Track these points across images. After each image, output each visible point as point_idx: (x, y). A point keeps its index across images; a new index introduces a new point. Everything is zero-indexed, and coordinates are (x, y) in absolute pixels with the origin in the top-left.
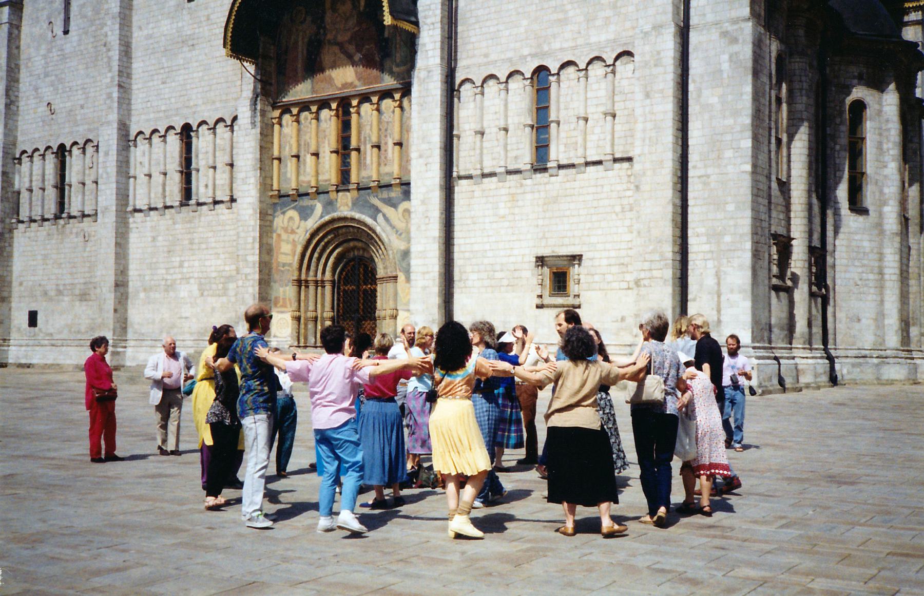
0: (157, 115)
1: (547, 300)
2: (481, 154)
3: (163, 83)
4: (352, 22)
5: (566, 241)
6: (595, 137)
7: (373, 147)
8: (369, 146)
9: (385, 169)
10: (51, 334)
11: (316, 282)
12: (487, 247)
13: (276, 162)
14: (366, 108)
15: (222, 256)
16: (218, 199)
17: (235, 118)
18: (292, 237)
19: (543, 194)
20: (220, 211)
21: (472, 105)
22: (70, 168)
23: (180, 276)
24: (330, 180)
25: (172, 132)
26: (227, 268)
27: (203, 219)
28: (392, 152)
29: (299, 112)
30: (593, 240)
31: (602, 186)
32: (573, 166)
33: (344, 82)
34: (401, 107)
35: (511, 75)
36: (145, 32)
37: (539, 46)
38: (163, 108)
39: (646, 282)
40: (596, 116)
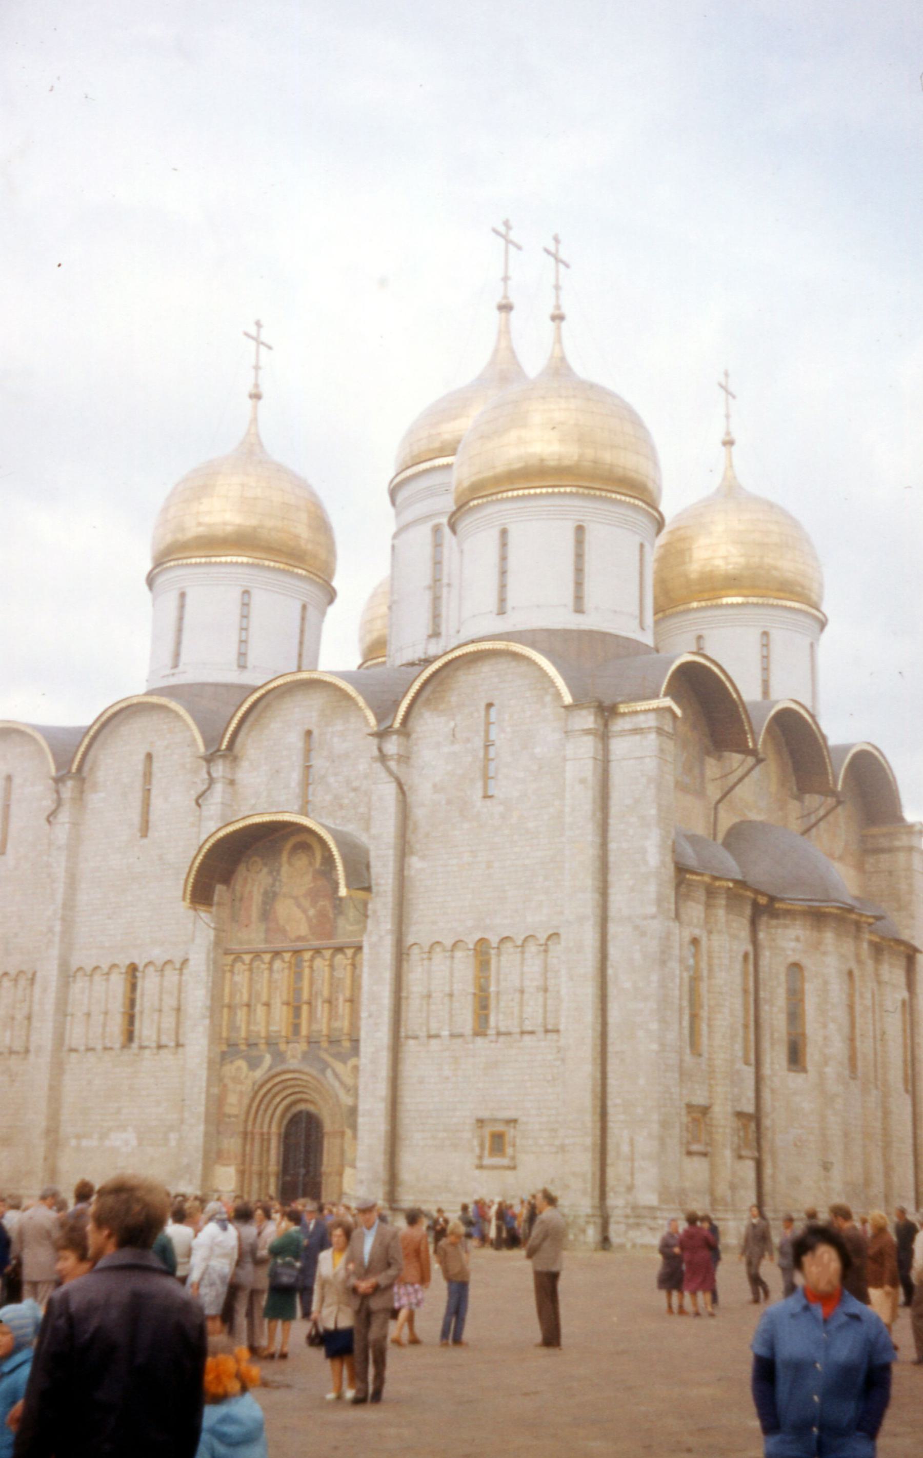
1: (487, 1161)
2: (428, 1017)
3: (109, 918)
4: (308, 878)
7: (324, 1002)
9: (337, 1024)
11: (262, 1134)
13: (225, 1010)
14: (319, 963)
17: (185, 961)
18: (239, 1087)
21: (420, 969)
25: (116, 970)
28: (343, 1008)
29: (252, 960)
34: (354, 966)
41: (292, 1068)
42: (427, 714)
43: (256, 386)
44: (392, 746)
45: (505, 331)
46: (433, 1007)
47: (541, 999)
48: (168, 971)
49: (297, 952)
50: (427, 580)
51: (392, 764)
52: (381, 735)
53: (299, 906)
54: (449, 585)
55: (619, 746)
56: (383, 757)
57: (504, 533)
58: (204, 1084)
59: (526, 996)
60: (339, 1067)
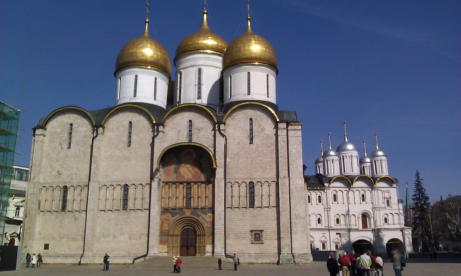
0: (112, 180)
3: (115, 170)
5: (259, 226)
6: (266, 201)
8: (197, 197)
10: (56, 252)
14: (196, 186)
15: (139, 227)
18: (168, 222)
19: (252, 214)
20: (139, 213)
24: (183, 205)
26: (141, 231)
27: (131, 215)
30: (267, 226)
31: (269, 213)
36: (108, 154)
37: (250, 176)
38: (115, 178)
39: (284, 238)
41: (188, 216)
42: (230, 120)
44: (222, 127)
49: (189, 183)
50: (197, 83)
52: (219, 123)
53: (188, 170)
54: (203, 85)
56: (219, 130)
60: (204, 216)
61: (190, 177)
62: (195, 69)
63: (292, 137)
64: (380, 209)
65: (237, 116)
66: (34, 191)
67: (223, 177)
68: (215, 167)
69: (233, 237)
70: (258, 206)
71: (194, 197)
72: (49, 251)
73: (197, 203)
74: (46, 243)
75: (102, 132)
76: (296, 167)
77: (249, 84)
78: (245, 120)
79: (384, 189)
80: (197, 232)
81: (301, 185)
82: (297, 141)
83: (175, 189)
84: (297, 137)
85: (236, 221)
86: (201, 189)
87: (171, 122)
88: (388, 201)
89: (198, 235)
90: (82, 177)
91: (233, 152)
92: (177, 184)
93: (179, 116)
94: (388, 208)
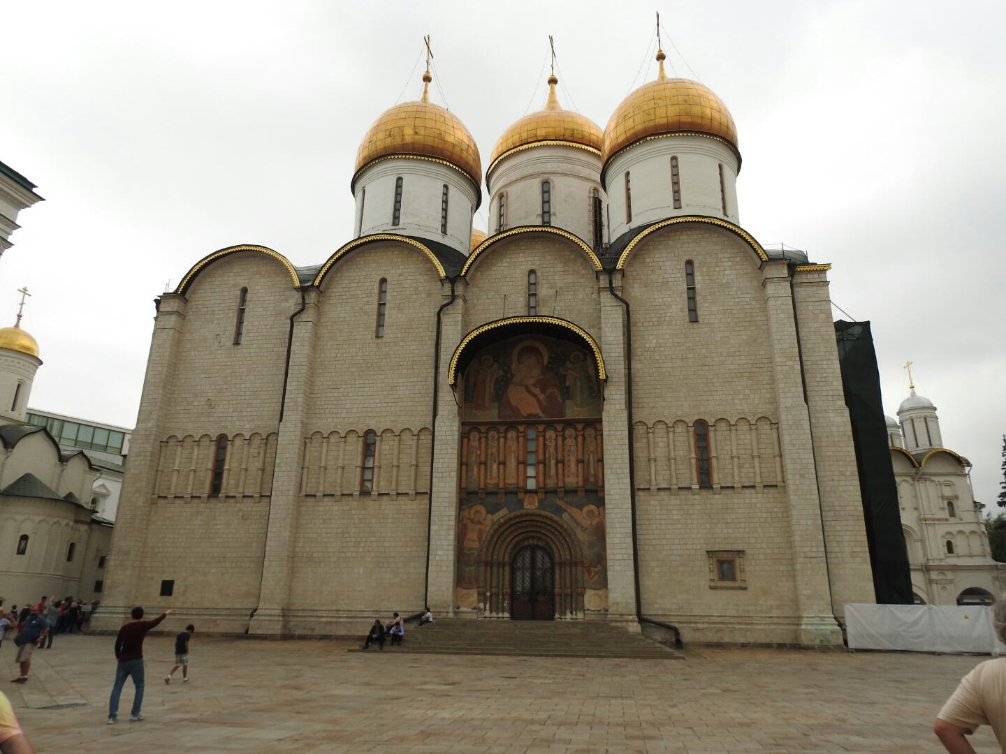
6: (746, 470)
7: (557, 464)
8: (553, 462)
12: (664, 542)
13: (464, 467)
14: (550, 434)
16: (400, 492)
18: (479, 526)
20: (402, 502)
22: (231, 458)
23: (354, 554)
24: (518, 484)
30: (753, 541)
32: (733, 487)
33: (529, 412)
35: (675, 423)
38: (343, 415)
40: (745, 456)
43: (427, 72)
45: (552, 93)
46: (659, 468)
47: (757, 464)
48: (406, 436)
50: (540, 212)
51: (619, 294)
54: (555, 214)
55: (801, 292)
57: (674, 158)
58: (453, 523)
59: (741, 461)
60: (576, 512)
61: (536, 410)
62: (536, 183)
63: (806, 304)
64: (936, 522)
65: (652, 256)
66: (146, 445)
67: (623, 407)
68: (602, 376)
69: (656, 570)
70: (724, 485)
71: (547, 462)
72: (176, 600)
73: (555, 477)
74: (167, 579)
75: (316, 303)
76: (823, 380)
77: (676, 183)
78: (676, 265)
79: (941, 479)
80: (557, 555)
81: (842, 428)
82: (818, 312)
83: (496, 442)
84: (820, 303)
85: (663, 527)
86: (566, 442)
87: (482, 275)
88: (950, 504)
89: (560, 564)
90: (264, 413)
91: (647, 346)
92: (502, 429)
93: (504, 260)
94: (952, 520)
